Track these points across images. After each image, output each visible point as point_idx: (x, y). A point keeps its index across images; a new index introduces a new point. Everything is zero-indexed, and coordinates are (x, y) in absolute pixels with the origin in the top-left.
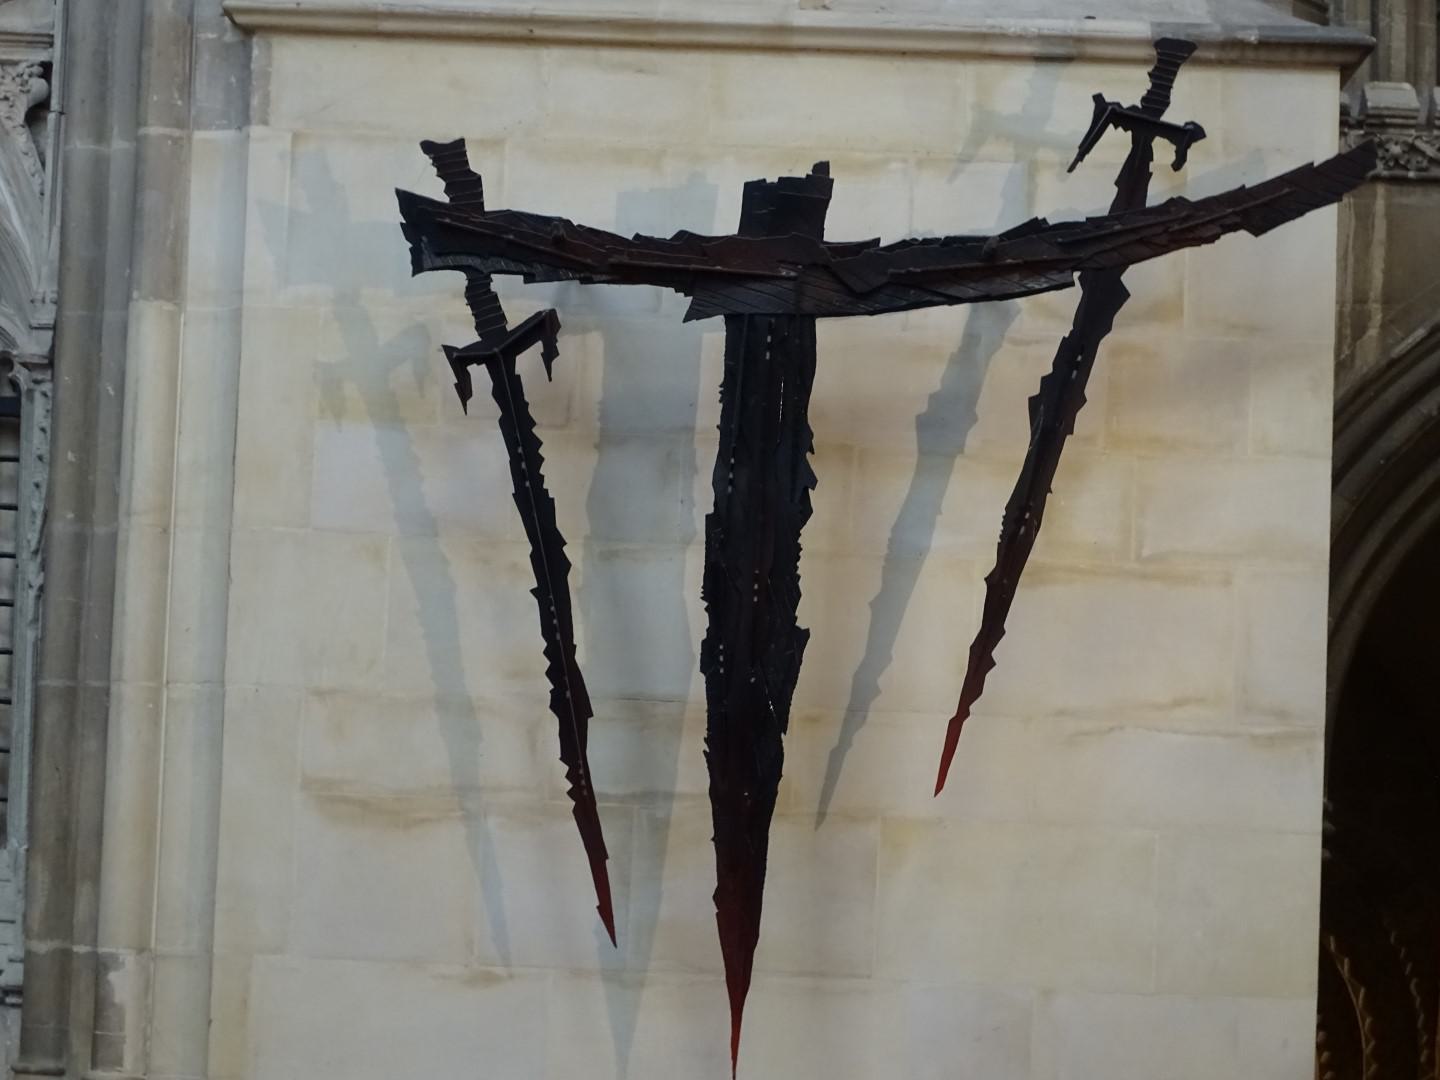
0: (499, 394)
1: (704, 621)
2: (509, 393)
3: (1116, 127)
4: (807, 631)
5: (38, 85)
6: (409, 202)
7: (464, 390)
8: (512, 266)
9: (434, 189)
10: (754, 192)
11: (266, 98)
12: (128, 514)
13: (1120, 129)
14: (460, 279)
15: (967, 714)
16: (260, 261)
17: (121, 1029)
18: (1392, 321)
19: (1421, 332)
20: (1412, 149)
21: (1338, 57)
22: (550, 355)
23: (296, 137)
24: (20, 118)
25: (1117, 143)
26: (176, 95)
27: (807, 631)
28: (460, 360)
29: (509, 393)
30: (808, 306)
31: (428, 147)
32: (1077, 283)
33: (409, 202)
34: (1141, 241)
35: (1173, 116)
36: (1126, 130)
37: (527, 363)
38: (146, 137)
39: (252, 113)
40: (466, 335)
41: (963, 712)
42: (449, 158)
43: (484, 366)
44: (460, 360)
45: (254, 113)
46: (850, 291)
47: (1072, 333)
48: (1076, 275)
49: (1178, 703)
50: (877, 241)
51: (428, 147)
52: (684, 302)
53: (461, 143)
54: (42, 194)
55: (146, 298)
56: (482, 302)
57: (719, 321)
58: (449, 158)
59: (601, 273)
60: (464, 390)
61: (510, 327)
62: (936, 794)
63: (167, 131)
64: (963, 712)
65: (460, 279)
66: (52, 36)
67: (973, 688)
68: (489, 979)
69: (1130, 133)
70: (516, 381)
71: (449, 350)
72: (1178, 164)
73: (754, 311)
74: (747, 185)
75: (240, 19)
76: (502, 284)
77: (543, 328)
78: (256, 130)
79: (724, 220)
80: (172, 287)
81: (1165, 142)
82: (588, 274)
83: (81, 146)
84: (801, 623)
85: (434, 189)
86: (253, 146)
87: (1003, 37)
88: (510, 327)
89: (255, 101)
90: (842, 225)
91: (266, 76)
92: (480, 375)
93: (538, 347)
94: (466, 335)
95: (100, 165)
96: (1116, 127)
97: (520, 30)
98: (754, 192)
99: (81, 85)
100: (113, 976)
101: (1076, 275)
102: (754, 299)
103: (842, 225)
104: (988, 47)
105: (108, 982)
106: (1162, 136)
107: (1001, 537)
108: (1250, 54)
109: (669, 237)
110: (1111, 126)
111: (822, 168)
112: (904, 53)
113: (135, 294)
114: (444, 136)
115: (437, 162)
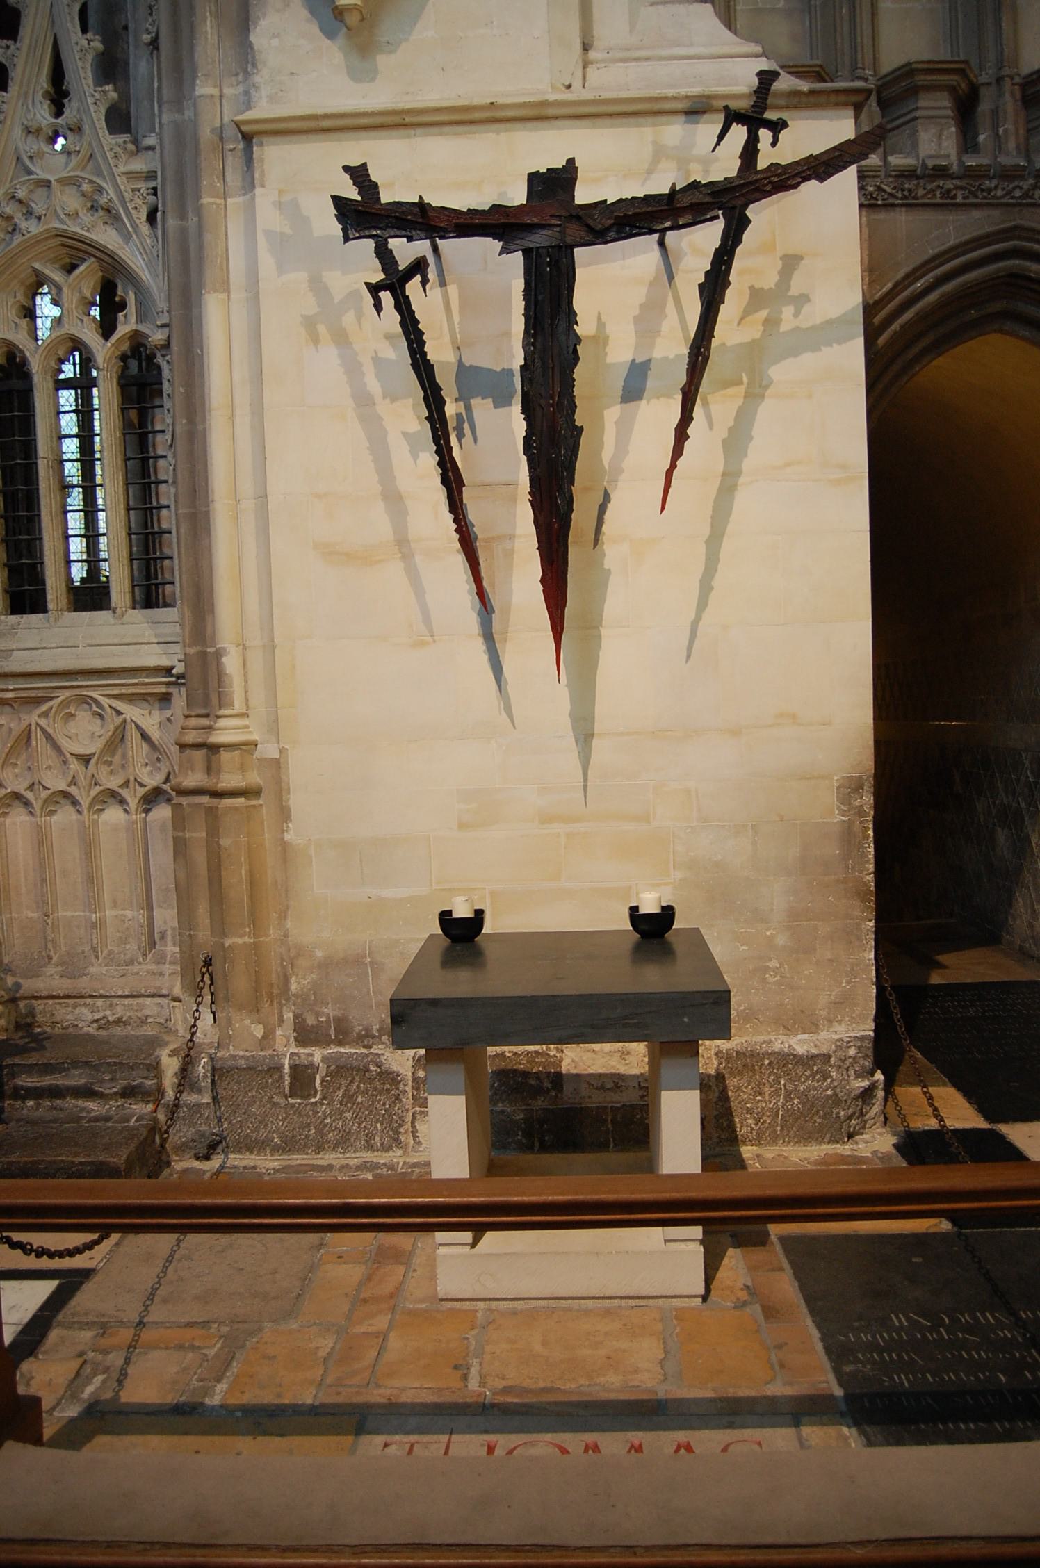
0: (398, 307)
1: (524, 426)
2: (403, 306)
3: (737, 124)
4: (582, 427)
5: (151, 198)
6: (338, 201)
7: (378, 306)
8: (398, 233)
9: (353, 194)
10: (533, 178)
11: (263, 172)
12: (210, 411)
13: (740, 125)
14: (370, 244)
15: (676, 466)
16: (266, 262)
17: (232, 687)
18: (874, 281)
19: (889, 285)
20: (879, 189)
21: (854, 98)
22: (424, 282)
23: (281, 192)
24: (144, 218)
25: (738, 134)
26: (216, 180)
27: (582, 427)
28: (374, 289)
29: (403, 306)
30: (569, 240)
31: (347, 169)
32: (721, 216)
33: (338, 201)
34: (757, 190)
35: (770, 115)
36: (743, 126)
37: (413, 288)
38: (202, 204)
39: (256, 182)
40: (378, 276)
41: (673, 465)
42: (359, 174)
43: (388, 292)
44: (374, 289)
46: (591, 230)
47: (720, 245)
48: (720, 212)
49: (788, 465)
50: (606, 201)
51: (347, 169)
52: (498, 245)
53: (365, 164)
54: (158, 256)
55: (209, 292)
56: (384, 255)
57: (519, 255)
58: (359, 174)
59: (450, 232)
60: (378, 306)
61: (401, 268)
63: (212, 200)
64: (673, 465)
65: (370, 244)
66: (156, 172)
67: (678, 451)
68: (422, 644)
69: (745, 127)
70: (407, 299)
72: (774, 143)
73: (538, 245)
74: (530, 175)
75: (244, 128)
76: (397, 244)
77: (419, 266)
78: (258, 191)
79: (517, 196)
80: (225, 286)
81: (766, 130)
82: (443, 234)
83: (172, 223)
84: (578, 423)
85: (353, 194)
86: (257, 200)
87: (666, 98)
88: (401, 268)
89: (257, 175)
90: (584, 195)
91: (262, 160)
92: (386, 297)
93: (418, 278)
94: (378, 276)
95: (183, 232)
96: (737, 124)
97: (397, 119)
98: (533, 178)
99: (170, 190)
100: (224, 659)
101: (720, 212)
102: (540, 239)
103: (584, 195)
104: (657, 106)
106: (764, 128)
107: (688, 365)
108: (804, 100)
109: (487, 209)
110: (734, 124)
111: (571, 162)
112: (611, 115)
113: (203, 292)
114: (354, 163)
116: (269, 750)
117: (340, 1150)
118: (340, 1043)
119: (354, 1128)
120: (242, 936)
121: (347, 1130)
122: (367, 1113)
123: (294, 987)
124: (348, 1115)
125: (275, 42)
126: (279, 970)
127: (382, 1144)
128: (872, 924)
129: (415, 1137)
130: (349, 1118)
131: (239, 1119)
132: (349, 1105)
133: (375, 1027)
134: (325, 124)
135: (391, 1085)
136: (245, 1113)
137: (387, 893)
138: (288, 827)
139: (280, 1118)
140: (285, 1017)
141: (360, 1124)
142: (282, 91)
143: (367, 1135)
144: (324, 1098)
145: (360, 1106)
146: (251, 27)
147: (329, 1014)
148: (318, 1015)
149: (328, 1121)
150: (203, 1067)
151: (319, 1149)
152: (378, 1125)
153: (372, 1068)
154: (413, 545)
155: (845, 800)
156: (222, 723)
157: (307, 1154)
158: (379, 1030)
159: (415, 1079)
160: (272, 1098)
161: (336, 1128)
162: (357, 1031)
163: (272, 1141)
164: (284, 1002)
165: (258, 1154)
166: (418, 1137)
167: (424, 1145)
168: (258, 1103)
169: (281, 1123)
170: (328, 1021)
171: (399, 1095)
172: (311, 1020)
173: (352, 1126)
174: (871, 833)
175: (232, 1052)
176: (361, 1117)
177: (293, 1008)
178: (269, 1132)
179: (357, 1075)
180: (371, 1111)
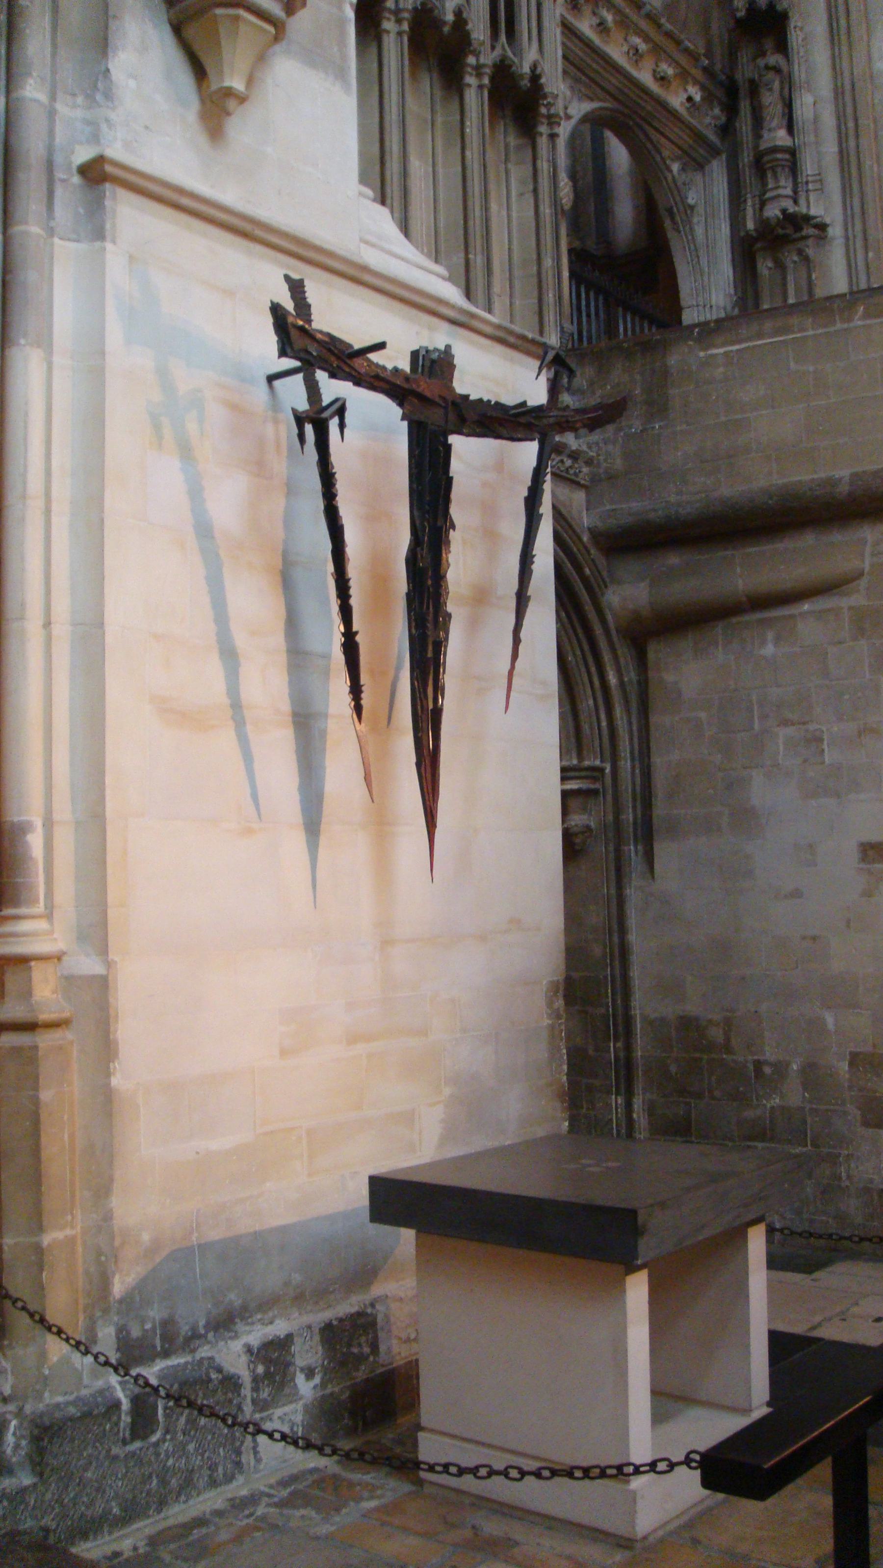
9: (289, 305)
40: (303, 405)
42: (297, 288)
44: (300, 420)
45: (108, 234)
50: (469, 396)
51: (287, 278)
58: (297, 288)
62: (505, 713)
71: (294, 411)
78: (109, 246)
80: (46, 343)
85: (289, 305)
94: (303, 405)
105: (26, 842)
114: (295, 276)
115: (290, 289)
116: (90, 966)
117: (183, 1498)
118: (166, 1354)
119: (197, 1463)
120: (62, 1228)
121: (191, 1469)
122: (209, 1437)
123: (118, 1288)
124: (191, 1447)
125: (132, 83)
126: (92, 1269)
127: (225, 1475)
128: (567, 1124)
129: (256, 1453)
130: (192, 1451)
131: (72, 1495)
132: (192, 1433)
133: (202, 1323)
134: (185, 201)
135: (233, 1393)
136: (79, 1484)
137: (215, 1145)
138: (115, 1068)
139: (119, 1476)
140: (100, 1335)
141: (202, 1455)
142: (136, 141)
143: (210, 1468)
144: (167, 1431)
145: (203, 1431)
146: (111, 54)
147: (154, 1319)
148: (143, 1322)
149: (170, 1462)
150: (14, 1434)
151: (162, 1504)
152: (221, 1450)
153: (214, 1376)
154: (245, 711)
155: (550, 1004)
156: (24, 926)
157: (149, 1517)
158: (206, 1326)
159: (256, 1380)
160: (111, 1450)
161: (179, 1468)
162: (183, 1333)
163: (110, 1513)
164: (99, 1314)
165: (95, 1539)
166: (259, 1452)
167: (264, 1461)
168: (94, 1464)
169: (120, 1484)
170: (154, 1329)
171: (241, 1403)
172: (136, 1333)
173: (195, 1461)
174: (563, 1034)
175: (47, 1401)
176: (204, 1445)
177: (116, 1319)
178: (107, 1501)
179: (200, 1389)
180: (214, 1434)
